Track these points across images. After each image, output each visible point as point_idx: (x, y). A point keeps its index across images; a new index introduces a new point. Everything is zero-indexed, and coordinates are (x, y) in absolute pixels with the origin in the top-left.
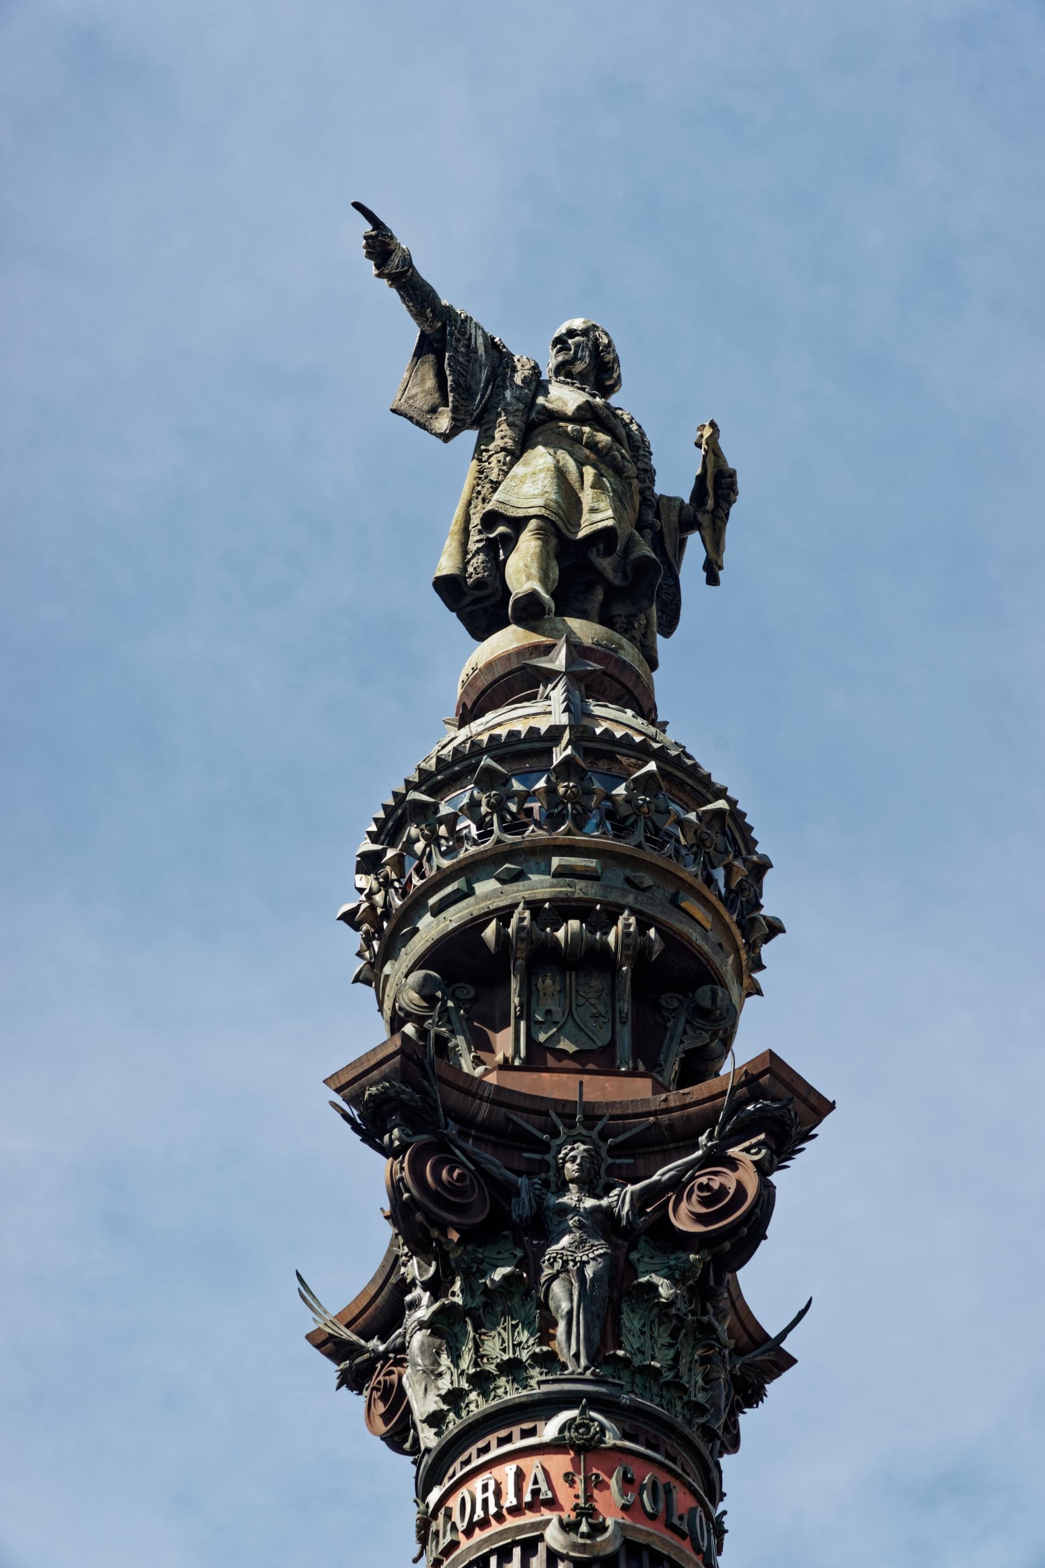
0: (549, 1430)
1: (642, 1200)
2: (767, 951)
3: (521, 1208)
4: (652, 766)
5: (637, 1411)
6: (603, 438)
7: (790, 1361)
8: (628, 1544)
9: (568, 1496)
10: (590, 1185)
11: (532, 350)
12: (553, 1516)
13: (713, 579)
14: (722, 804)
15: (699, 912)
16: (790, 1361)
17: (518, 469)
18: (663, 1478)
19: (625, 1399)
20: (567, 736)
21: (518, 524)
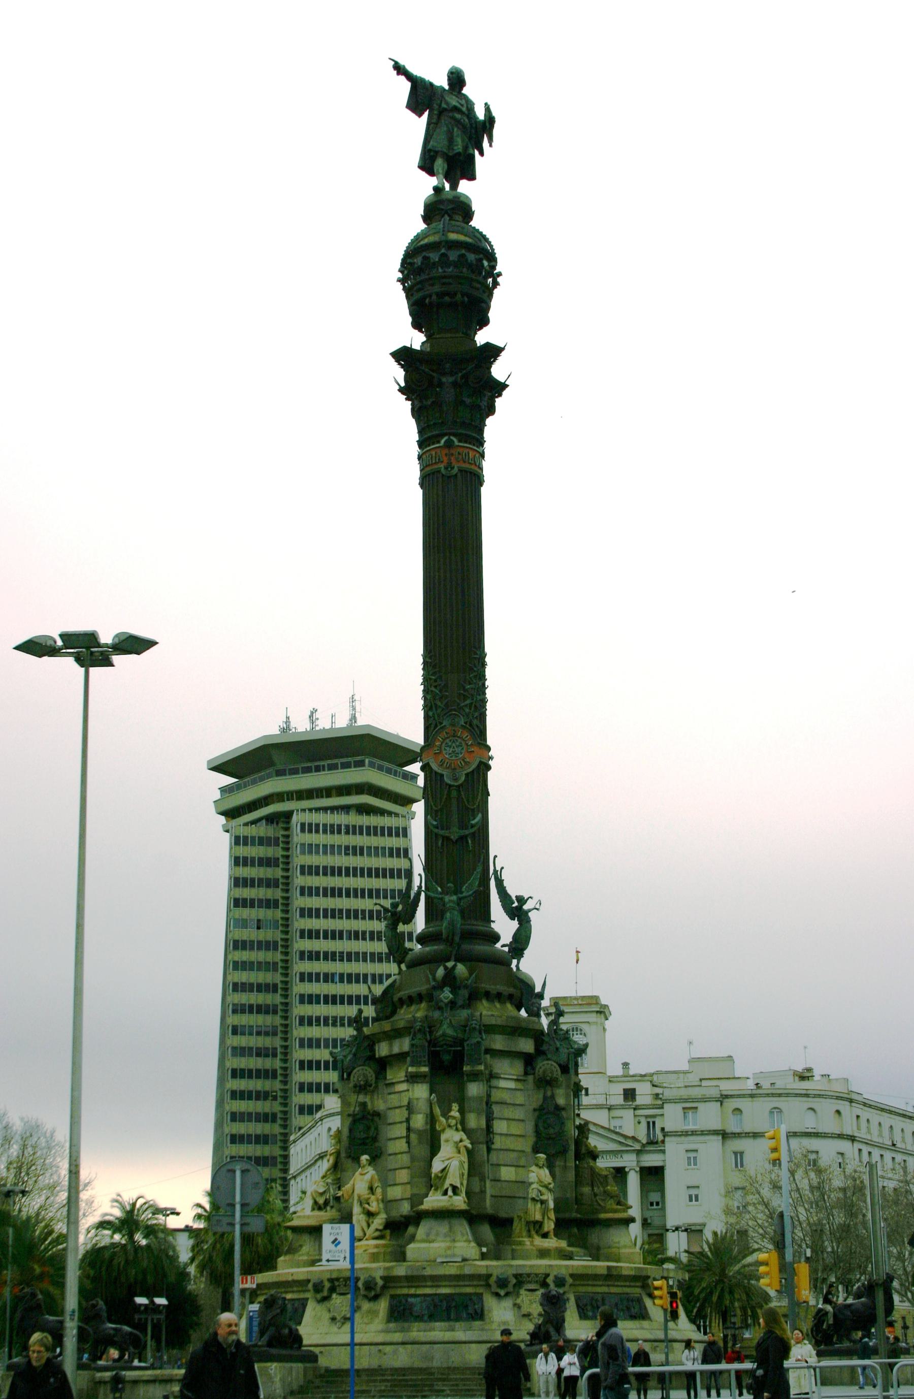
0: (443, 441)
1: (462, 378)
2: (499, 279)
3: (435, 381)
4: (463, 251)
5: (461, 434)
6: (458, 116)
7: (508, 386)
8: (460, 470)
9: (445, 459)
10: (451, 374)
11: (441, 81)
12: (442, 466)
13: (491, 146)
14: (481, 256)
15: (478, 286)
16: (508, 386)
17: (438, 130)
18: (466, 451)
19: (460, 431)
20: (443, 244)
21: (436, 152)
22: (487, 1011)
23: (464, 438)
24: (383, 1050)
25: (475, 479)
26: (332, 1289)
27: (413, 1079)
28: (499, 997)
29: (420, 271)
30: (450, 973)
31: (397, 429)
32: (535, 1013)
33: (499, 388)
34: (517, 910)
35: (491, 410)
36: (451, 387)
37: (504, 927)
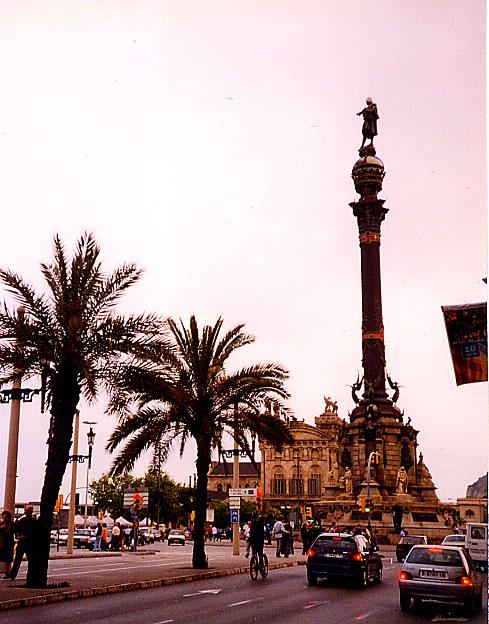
22: (385, 420)
23: (373, 231)
24: (351, 432)
25: (378, 244)
26: (335, 509)
27: (360, 442)
28: (389, 416)
29: (359, 174)
30: (371, 408)
31: (349, 226)
32: (401, 420)
33: (386, 211)
34: (396, 388)
35: (384, 218)
36: (369, 213)
37: (390, 392)
